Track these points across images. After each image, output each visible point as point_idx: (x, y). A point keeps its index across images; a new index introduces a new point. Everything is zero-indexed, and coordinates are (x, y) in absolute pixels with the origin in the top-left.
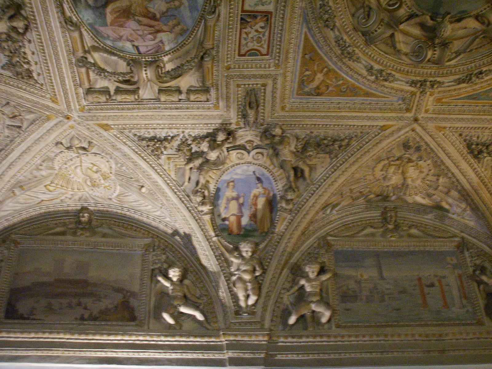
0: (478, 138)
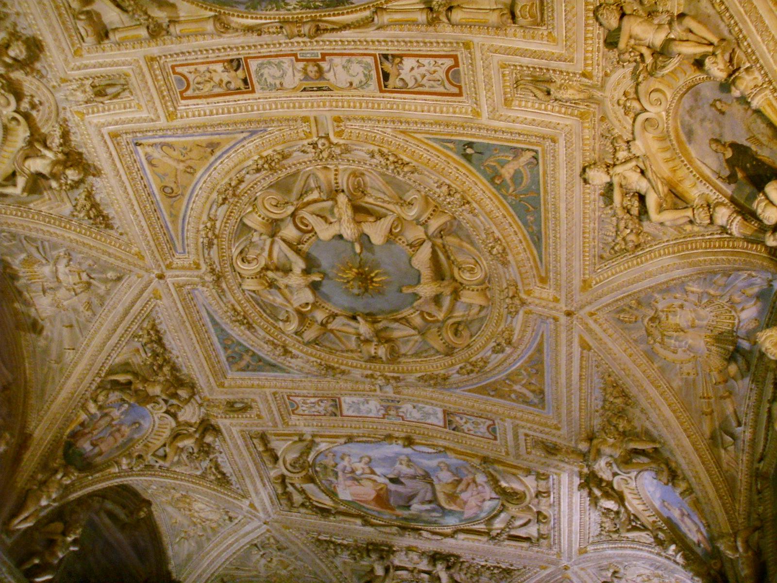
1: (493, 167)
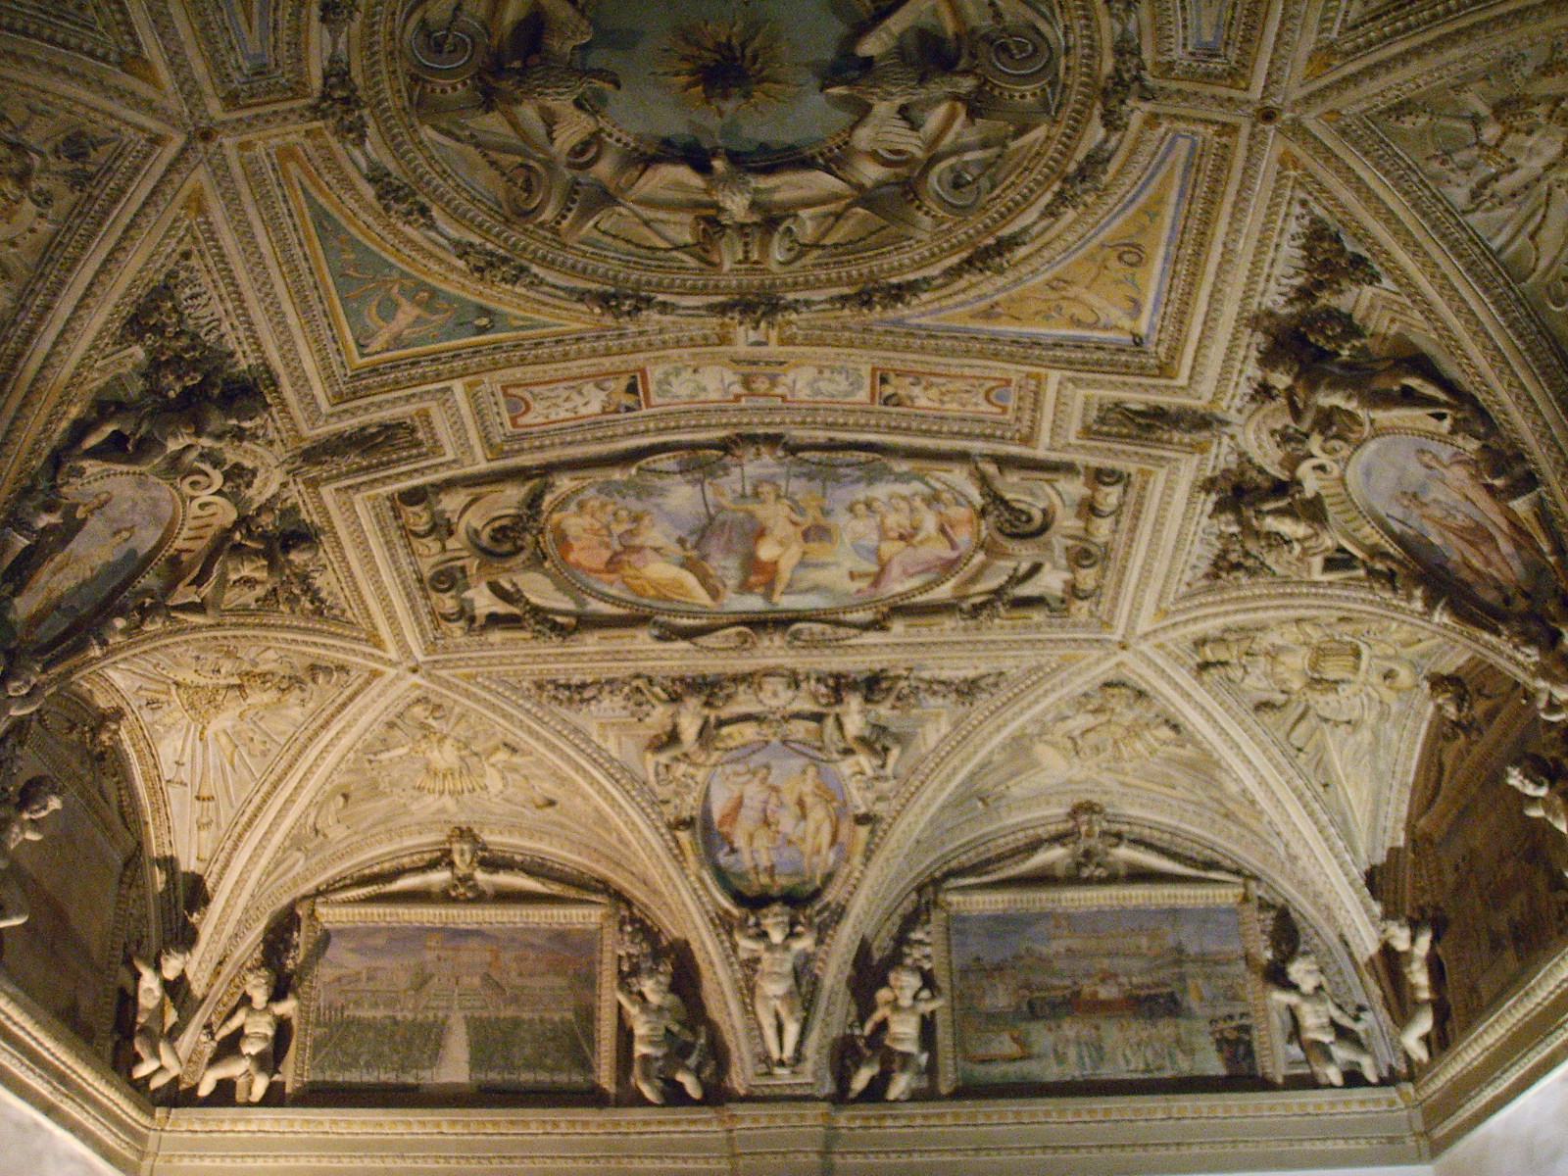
0: (193, 297)
1: (435, 312)
